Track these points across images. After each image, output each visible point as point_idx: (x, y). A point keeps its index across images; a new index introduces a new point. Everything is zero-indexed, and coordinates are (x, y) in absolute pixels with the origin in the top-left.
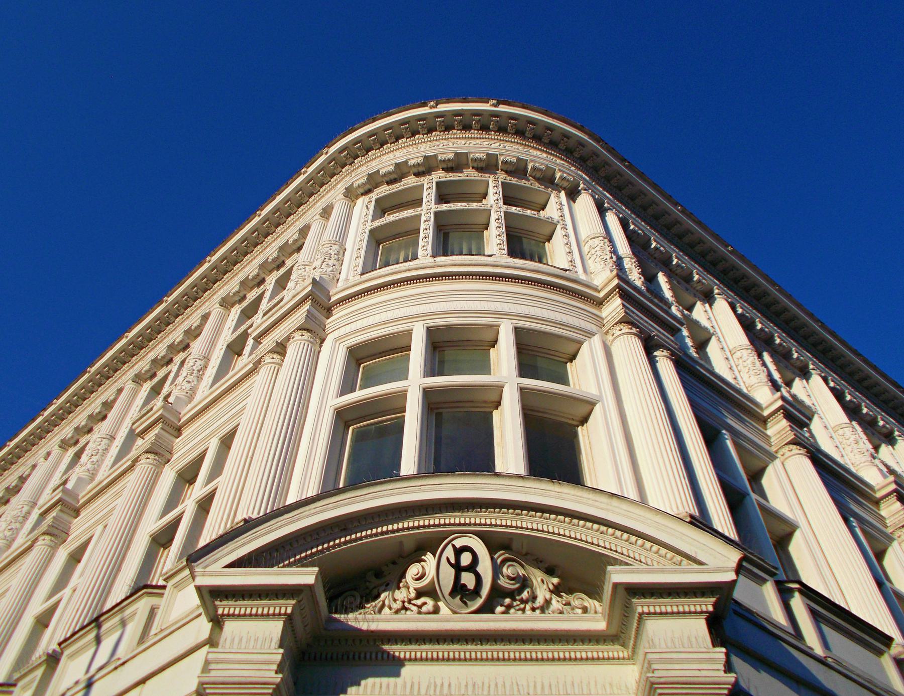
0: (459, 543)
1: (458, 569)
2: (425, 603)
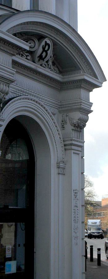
0: (48, 42)
1: (44, 48)
2: (28, 56)
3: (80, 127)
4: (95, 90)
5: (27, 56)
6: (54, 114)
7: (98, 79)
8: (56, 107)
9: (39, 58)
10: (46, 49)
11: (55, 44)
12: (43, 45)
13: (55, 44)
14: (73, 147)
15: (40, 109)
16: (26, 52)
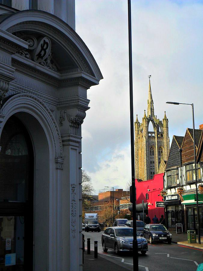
0: (47, 40)
2: (28, 54)
3: (77, 123)
4: (92, 88)
5: (26, 54)
6: (52, 111)
7: (95, 77)
8: (54, 104)
9: (37, 57)
10: (45, 47)
11: (53, 43)
12: (42, 44)
13: (53, 43)
14: (71, 143)
15: (38, 106)
16: (25, 51)
